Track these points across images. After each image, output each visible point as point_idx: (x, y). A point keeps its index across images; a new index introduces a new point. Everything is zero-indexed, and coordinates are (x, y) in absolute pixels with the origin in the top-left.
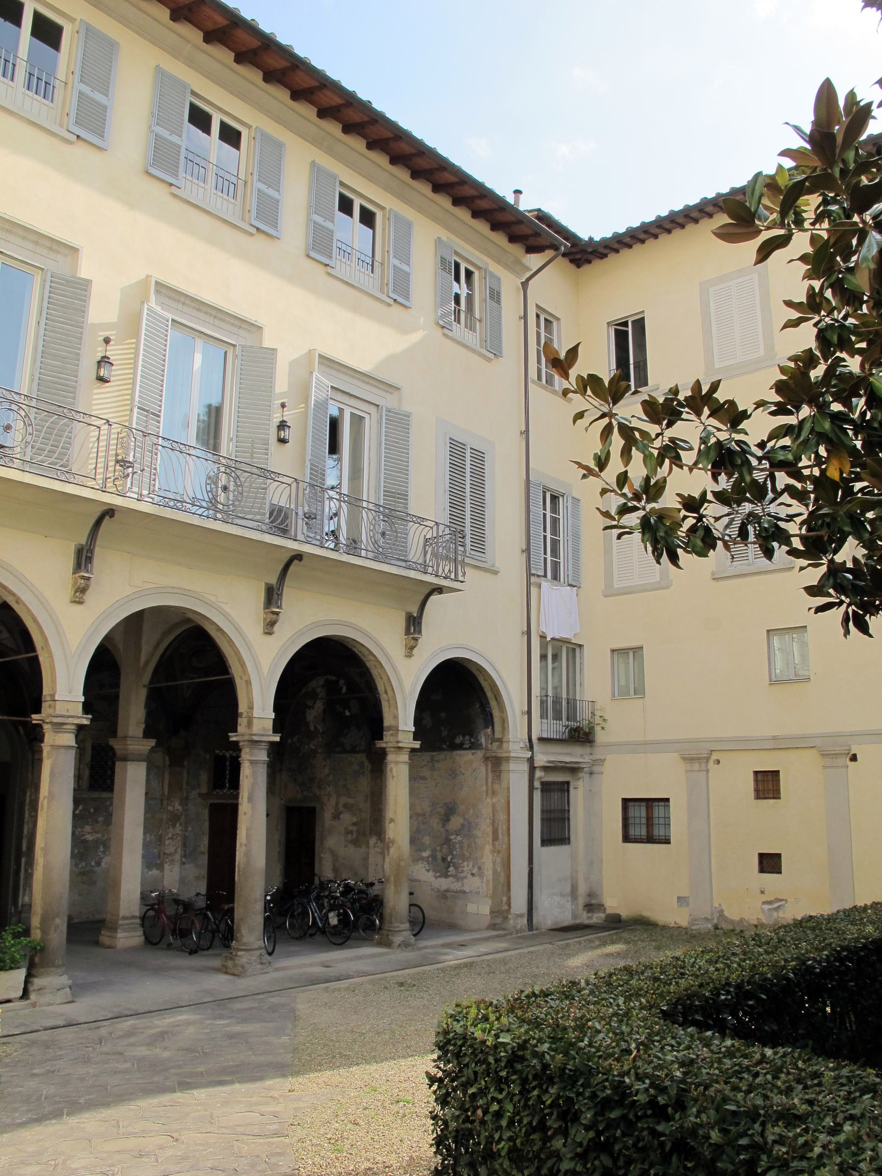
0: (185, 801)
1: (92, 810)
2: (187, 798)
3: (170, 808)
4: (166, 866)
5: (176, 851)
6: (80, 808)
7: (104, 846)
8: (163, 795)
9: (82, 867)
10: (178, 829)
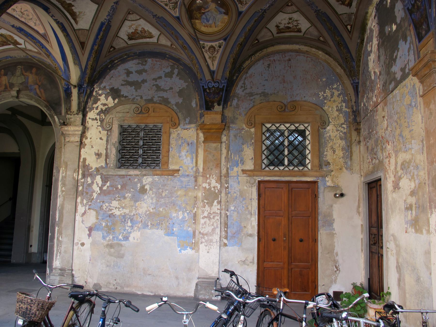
0: (224, 178)
1: (119, 187)
2: (227, 175)
3: (206, 185)
4: (202, 246)
5: (214, 230)
6: (108, 184)
7: (132, 220)
8: (197, 171)
9: (109, 240)
10: (216, 207)
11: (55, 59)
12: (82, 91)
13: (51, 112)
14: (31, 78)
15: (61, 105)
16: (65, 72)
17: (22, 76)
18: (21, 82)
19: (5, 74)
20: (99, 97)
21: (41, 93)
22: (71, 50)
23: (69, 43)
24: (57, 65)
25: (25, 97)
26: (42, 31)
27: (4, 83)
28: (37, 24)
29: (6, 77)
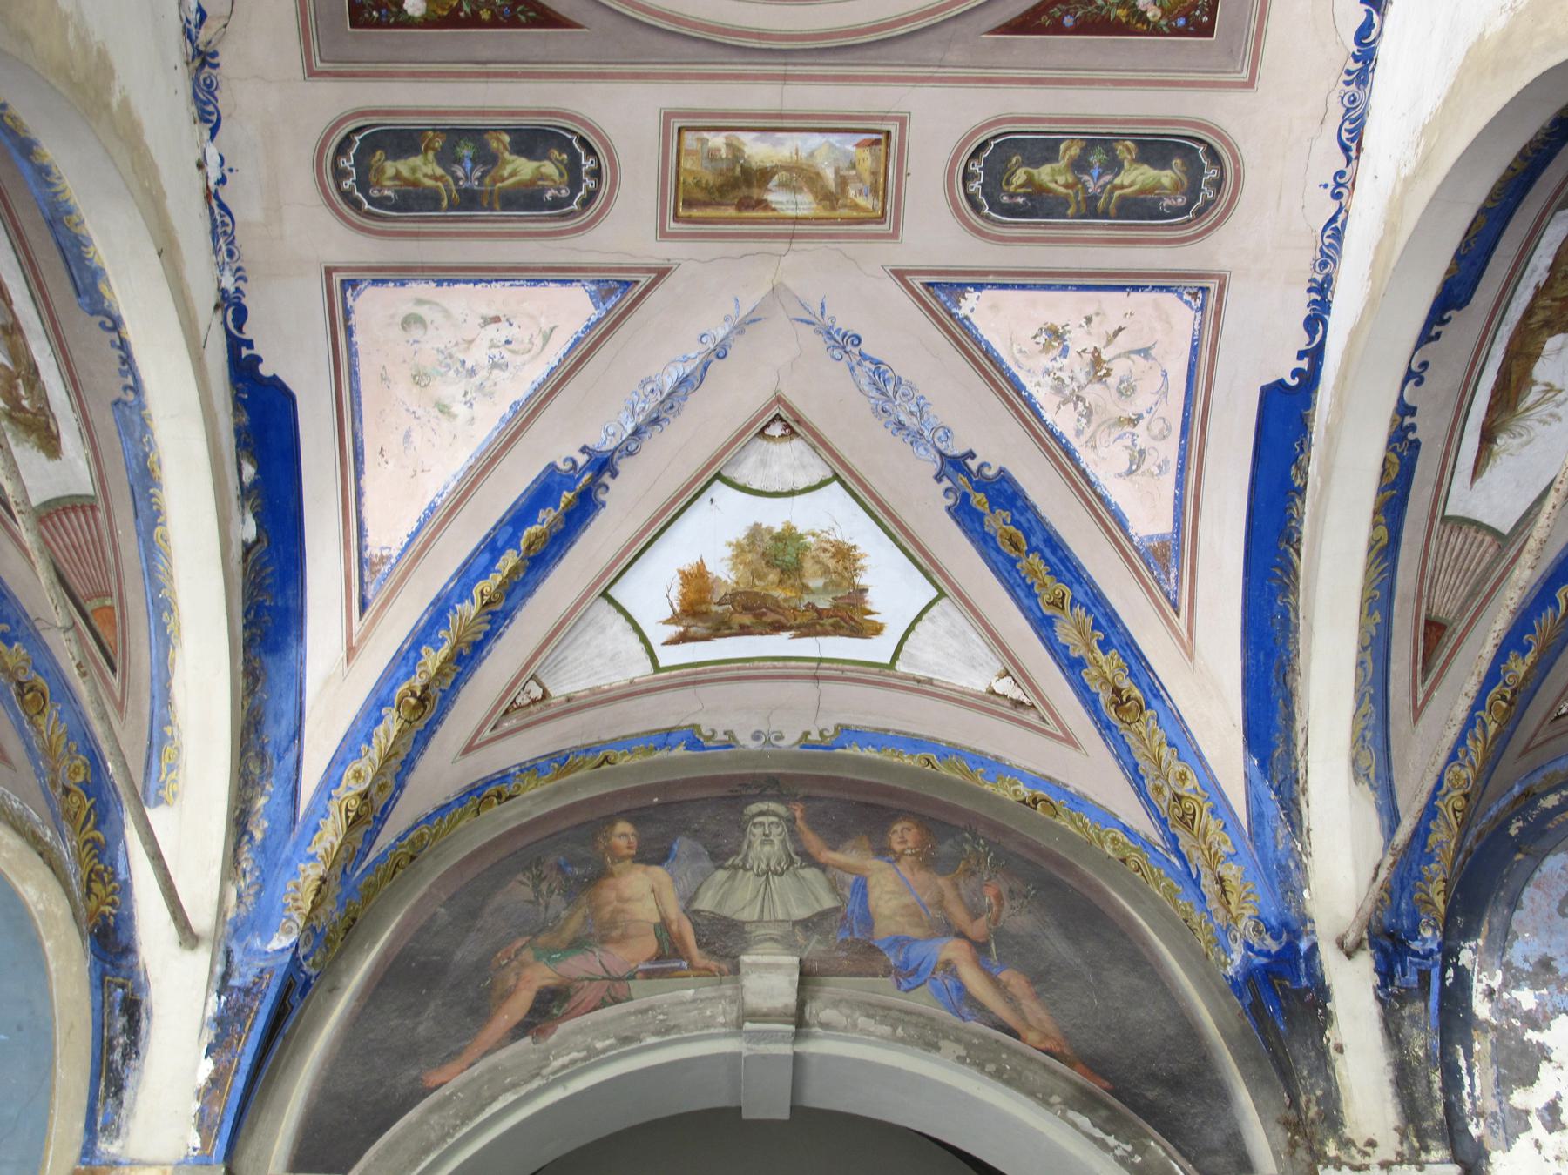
11: (1186, 730)
12: (1412, 978)
13: (1141, 1149)
14: (893, 890)
15: (1222, 1095)
16: (1255, 836)
17: (810, 873)
18: (800, 913)
19: (653, 854)
20: (1531, 1035)
21: (1011, 1000)
22: (1361, 664)
23: (1370, 613)
24: (1192, 782)
25: (862, 1021)
26: (1149, 517)
27: (645, 911)
28: (1149, 464)
29: (657, 871)
